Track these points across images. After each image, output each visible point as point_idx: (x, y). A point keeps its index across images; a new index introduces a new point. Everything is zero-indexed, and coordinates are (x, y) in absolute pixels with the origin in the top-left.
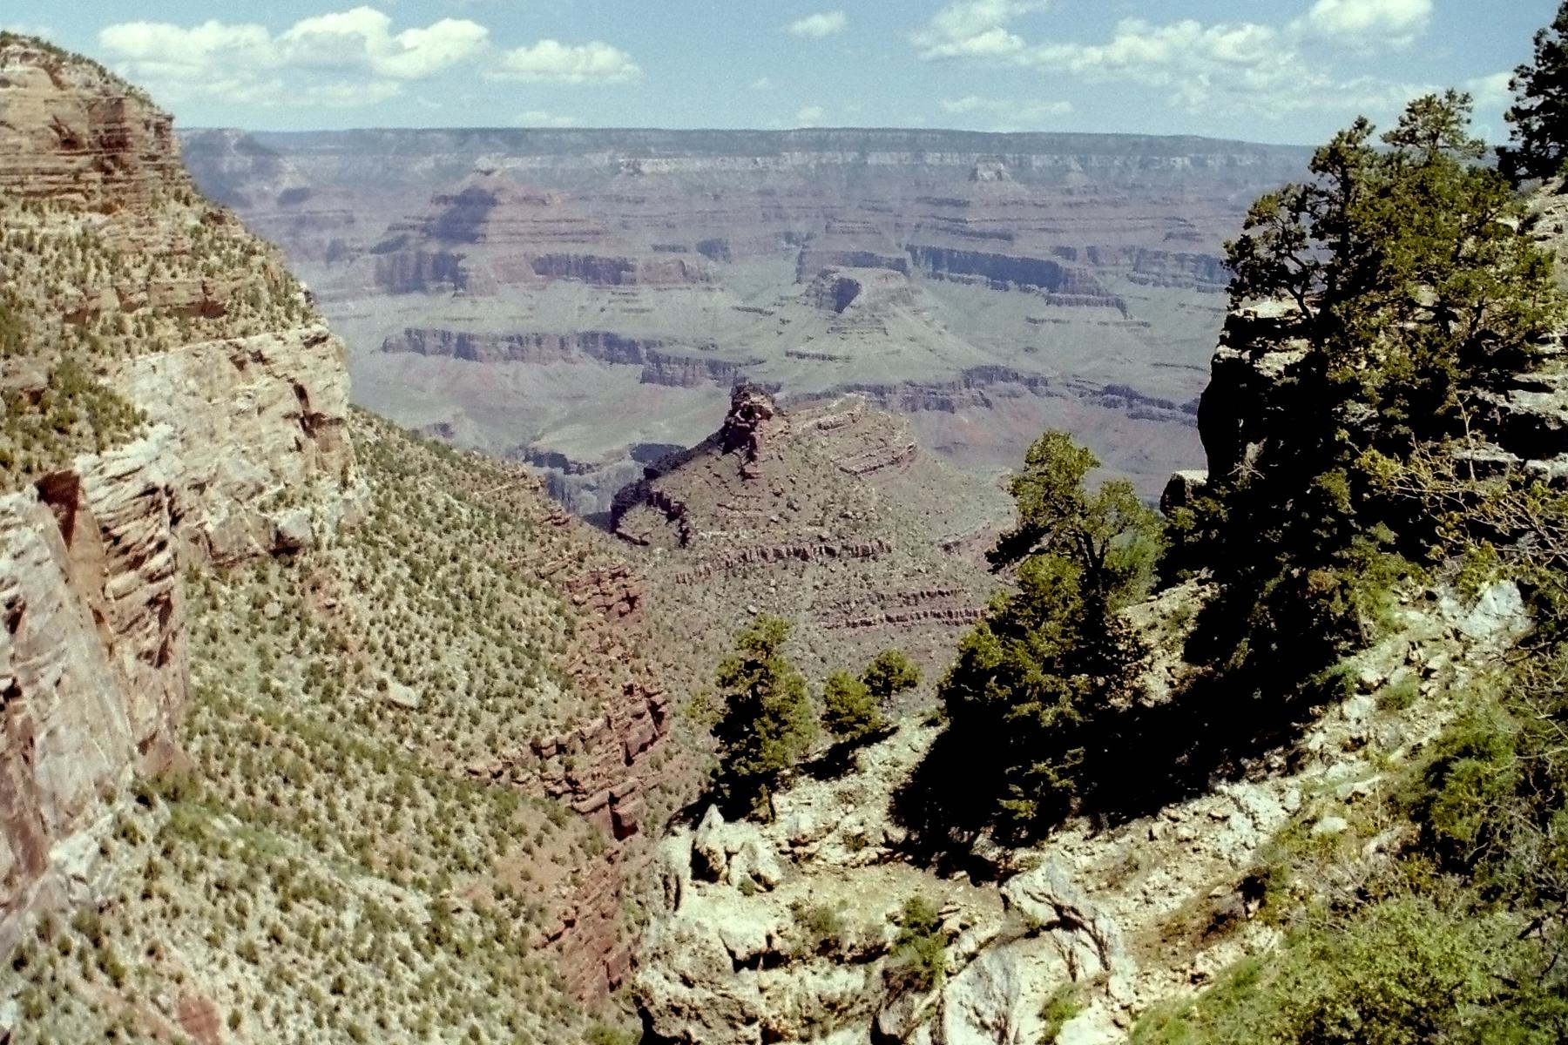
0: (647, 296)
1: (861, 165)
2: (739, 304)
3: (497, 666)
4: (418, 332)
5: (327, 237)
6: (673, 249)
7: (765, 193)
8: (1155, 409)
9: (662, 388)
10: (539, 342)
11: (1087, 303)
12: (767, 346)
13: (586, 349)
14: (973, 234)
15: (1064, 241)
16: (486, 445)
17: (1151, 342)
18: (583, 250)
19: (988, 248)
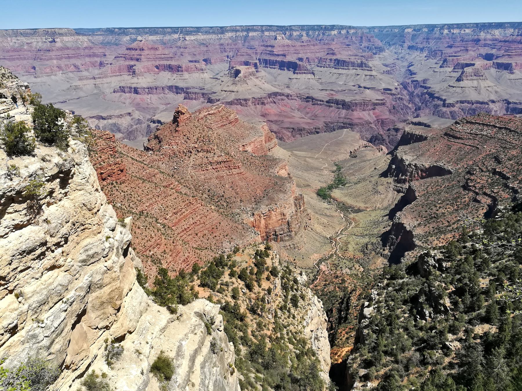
0: (186, 75)
1: (247, 36)
4: (123, 87)
5: (98, 60)
6: (196, 61)
7: (222, 45)
8: (319, 102)
9: (189, 101)
10: (156, 89)
11: (305, 73)
12: (217, 89)
13: (170, 90)
14: (276, 55)
15: (300, 56)
16: (141, 118)
17: (321, 83)
18: (168, 63)
19: (279, 59)
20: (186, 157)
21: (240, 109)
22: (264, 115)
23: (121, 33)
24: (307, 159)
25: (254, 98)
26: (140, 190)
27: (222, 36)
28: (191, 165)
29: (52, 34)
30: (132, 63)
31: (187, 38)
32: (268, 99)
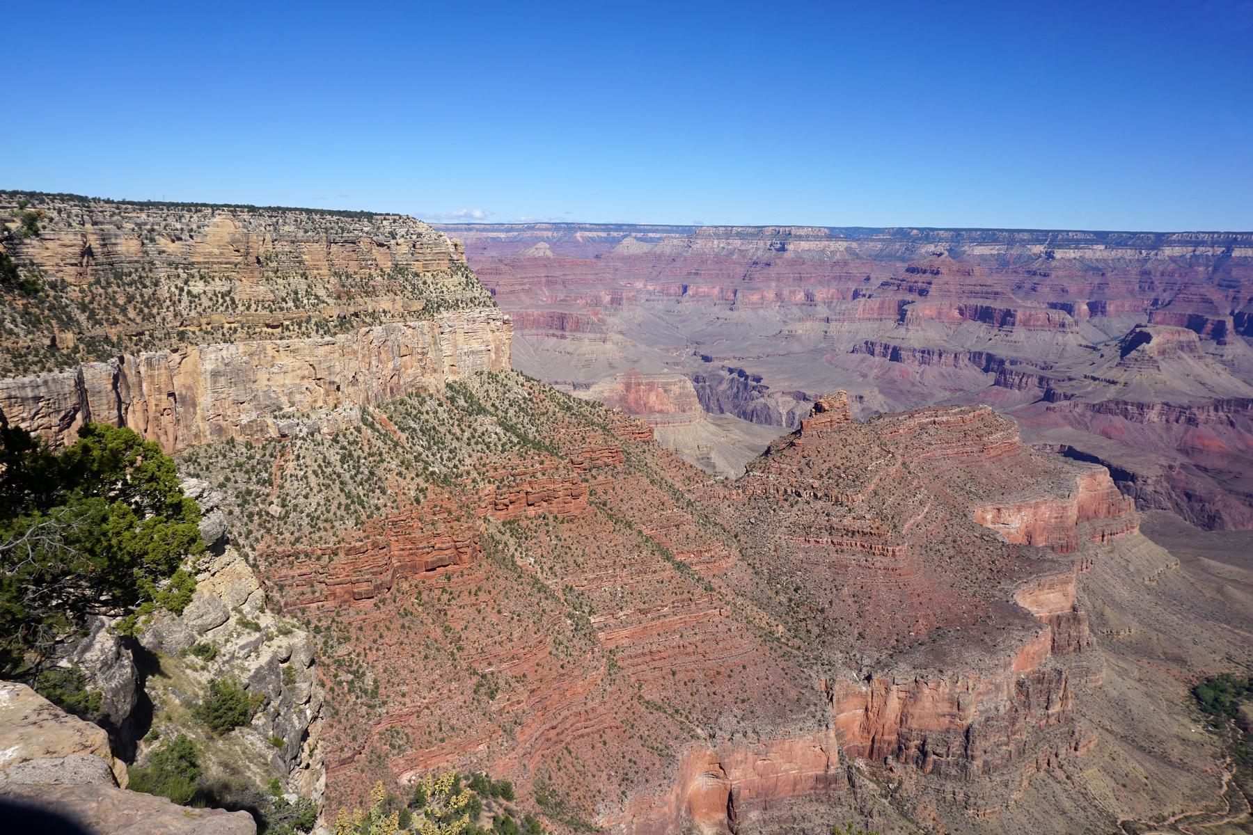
2: (1084, 343)
3: (333, 508)
7: (1146, 273)
13: (974, 362)
18: (986, 303)
20: (786, 505)
21: (1119, 425)
22: (1184, 451)
23: (920, 239)
24: (1230, 589)
25: (1167, 404)
26: (595, 544)
27: (1153, 253)
28: (786, 524)
29: (782, 237)
30: (909, 297)
31: (1058, 254)
32: (1212, 413)
